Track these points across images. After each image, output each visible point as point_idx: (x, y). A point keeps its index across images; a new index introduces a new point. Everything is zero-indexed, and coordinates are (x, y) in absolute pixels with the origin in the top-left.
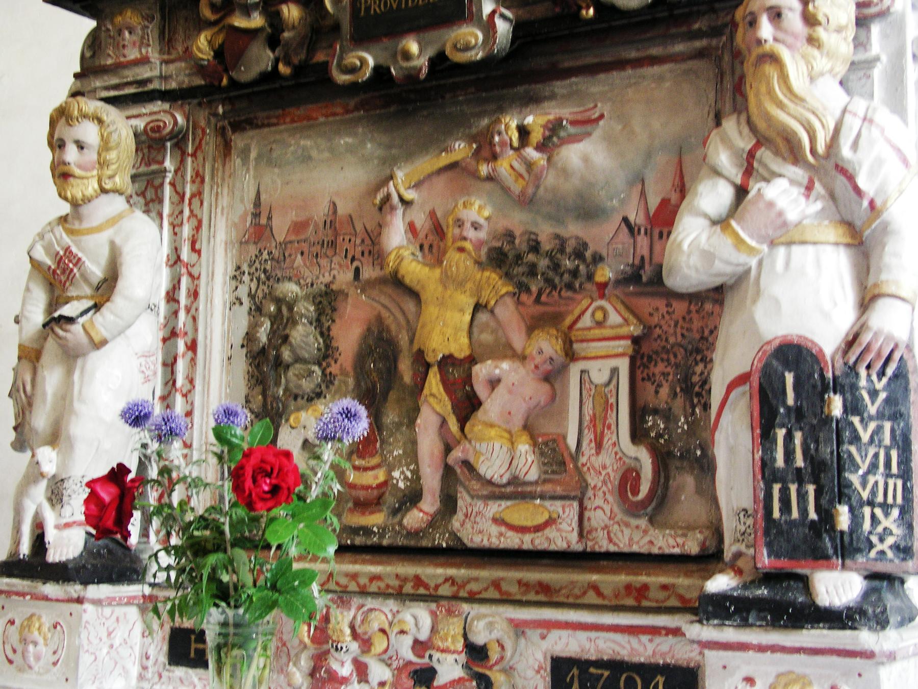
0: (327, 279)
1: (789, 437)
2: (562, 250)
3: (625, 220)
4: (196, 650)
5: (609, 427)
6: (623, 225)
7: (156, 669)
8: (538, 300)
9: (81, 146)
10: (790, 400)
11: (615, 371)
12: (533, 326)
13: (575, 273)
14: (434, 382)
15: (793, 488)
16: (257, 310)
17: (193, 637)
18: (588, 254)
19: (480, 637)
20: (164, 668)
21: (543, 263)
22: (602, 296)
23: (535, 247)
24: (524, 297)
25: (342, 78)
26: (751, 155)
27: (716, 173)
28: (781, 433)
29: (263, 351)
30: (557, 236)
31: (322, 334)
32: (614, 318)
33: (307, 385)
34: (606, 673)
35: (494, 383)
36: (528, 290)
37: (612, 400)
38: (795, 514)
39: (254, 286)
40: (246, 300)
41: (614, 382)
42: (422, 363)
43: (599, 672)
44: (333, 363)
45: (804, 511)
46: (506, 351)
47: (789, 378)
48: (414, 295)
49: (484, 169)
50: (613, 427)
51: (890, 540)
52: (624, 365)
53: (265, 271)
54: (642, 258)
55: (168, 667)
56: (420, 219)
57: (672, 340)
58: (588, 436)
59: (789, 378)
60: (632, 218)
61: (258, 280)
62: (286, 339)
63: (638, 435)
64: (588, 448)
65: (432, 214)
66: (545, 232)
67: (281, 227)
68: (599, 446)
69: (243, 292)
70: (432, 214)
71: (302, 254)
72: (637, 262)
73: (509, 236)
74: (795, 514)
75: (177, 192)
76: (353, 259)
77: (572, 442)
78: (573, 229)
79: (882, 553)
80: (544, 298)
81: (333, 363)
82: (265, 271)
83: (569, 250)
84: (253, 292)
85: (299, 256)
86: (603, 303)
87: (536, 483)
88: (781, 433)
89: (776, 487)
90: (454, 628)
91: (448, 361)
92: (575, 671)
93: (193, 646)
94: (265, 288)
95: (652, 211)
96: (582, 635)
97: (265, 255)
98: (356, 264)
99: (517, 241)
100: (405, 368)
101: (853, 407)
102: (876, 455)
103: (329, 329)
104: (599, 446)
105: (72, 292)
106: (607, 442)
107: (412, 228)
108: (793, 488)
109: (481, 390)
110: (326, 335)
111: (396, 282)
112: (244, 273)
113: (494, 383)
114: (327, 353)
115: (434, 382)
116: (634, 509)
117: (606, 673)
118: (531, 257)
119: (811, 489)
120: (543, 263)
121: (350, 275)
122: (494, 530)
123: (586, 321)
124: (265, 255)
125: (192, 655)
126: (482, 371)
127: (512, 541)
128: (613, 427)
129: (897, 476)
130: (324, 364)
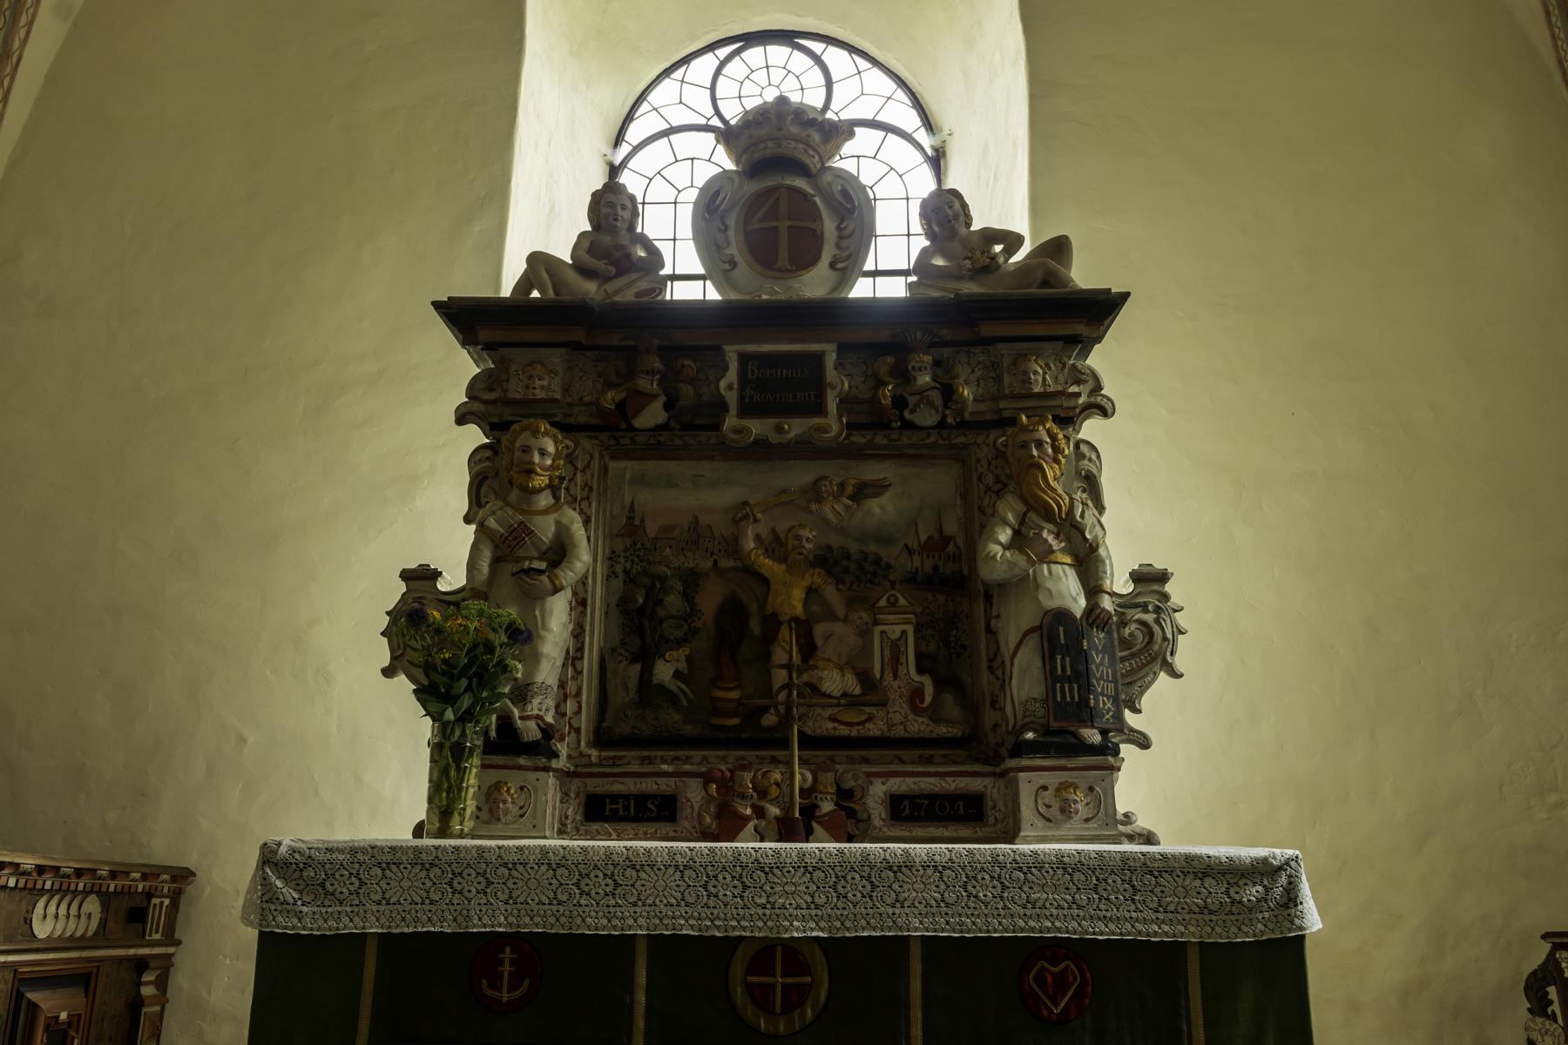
0: (692, 565)
1: (1063, 660)
2: (865, 560)
3: (906, 546)
4: (611, 810)
5: (902, 664)
6: (905, 549)
7: (574, 825)
8: (850, 588)
9: (543, 453)
10: (1063, 642)
11: (904, 632)
12: (851, 603)
13: (875, 574)
14: (784, 632)
15: (1067, 686)
16: (631, 580)
17: (608, 800)
18: (883, 564)
19: (849, 783)
20: (582, 824)
21: (853, 567)
22: (893, 589)
23: (848, 557)
24: (841, 586)
26: (1025, 514)
27: (1006, 523)
28: (1059, 657)
29: (641, 610)
30: (862, 552)
31: (688, 601)
32: (902, 601)
34: (927, 802)
35: (828, 637)
36: (844, 583)
37: (903, 649)
38: (1068, 699)
39: (628, 565)
40: (621, 575)
41: (904, 636)
42: (772, 623)
43: (922, 801)
44: (696, 620)
45: (1072, 697)
46: (831, 616)
47: (1061, 629)
48: (765, 581)
49: (814, 507)
50: (904, 664)
51: (1111, 714)
52: (910, 629)
53: (638, 556)
54: (917, 569)
55: (584, 823)
56: (764, 532)
57: (936, 616)
58: (888, 671)
59: (1061, 629)
60: (910, 544)
61: (633, 562)
62: (660, 602)
63: (920, 671)
64: (889, 678)
65: (773, 531)
66: (854, 547)
67: (652, 529)
68: (895, 676)
69: (619, 568)
70: (773, 531)
71: (670, 547)
72: (914, 570)
73: (829, 548)
74: (1068, 699)
75: (571, 495)
76: (712, 554)
77: (877, 673)
78: (873, 548)
79: (1108, 719)
80: (854, 587)
81: (696, 620)
82: (638, 556)
83: (870, 560)
84: (628, 569)
85: (668, 549)
86: (894, 592)
87: (859, 696)
88: (1059, 657)
89: (1058, 685)
90: (829, 778)
92: (906, 802)
93: (608, 807)
94: (639, 568)
95: (923, 541)
96: (910, 780)
97: (639, 546)
98: (714, 557)
99: (835, 552)
100: (755, 626)
101: (1092, 645)
102: (1102, 671)
103: (693, 598)
104: (895, 676)
105: (521, 553)
106: (902, 671)
107: (758, 538)
108: (1067, 686)
110: (690, 601)
112: (619, 556)
116: (917, 711)
117: (927, 802)
118: (845, 562)
119: (1076, 686)
120: (853, 567)
121: (710, 564)
122: (830, 725)
123: (883, 603)
124: (639, 546)
125: (607, 813)
126: (820, 630)
127: (844, 731)
128: (904, 664)
129: (1111, 682)
130: (690, 621)
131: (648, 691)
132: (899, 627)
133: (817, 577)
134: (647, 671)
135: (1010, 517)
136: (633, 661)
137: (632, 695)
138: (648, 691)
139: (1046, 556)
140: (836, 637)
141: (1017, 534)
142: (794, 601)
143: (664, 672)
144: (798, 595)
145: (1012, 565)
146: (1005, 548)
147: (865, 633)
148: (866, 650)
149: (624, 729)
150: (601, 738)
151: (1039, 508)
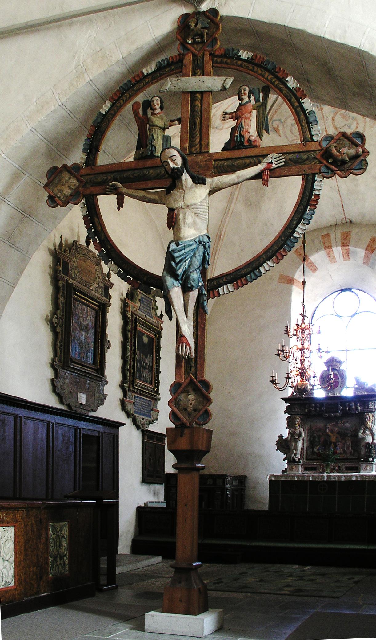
12: (342, 439)
14: (332, 444)
23: (342, 432)
25: (324, 416)
27: (362, 430)
32: (350, 439)
33: (317, 444)
35: (339, 444)
42: (331, 443)
78: (346, 431)
91: (334, 443)
109: (337, 445)
111: (328, 435)
113: (339, 444)
114: (319, 441)
115: (332, 444)
131: (313, 452)
132: (349, 443)
133: (338, 436)
134: (313, 450)
135: (362, 428)
136: (311, 448)
137: (311, 453)
138: (313, 452)
139: (368, 435)
140: (340, 445)
141: (364, 431)
142: (333, 440)
143: (315, 450)
144: (335, 438)
145: (362, 436)
146: (362, 433)
147: (344, 444)
148: (344, 446)
149: (310, 458)
150: (307, 459)
151: (366, 428)
